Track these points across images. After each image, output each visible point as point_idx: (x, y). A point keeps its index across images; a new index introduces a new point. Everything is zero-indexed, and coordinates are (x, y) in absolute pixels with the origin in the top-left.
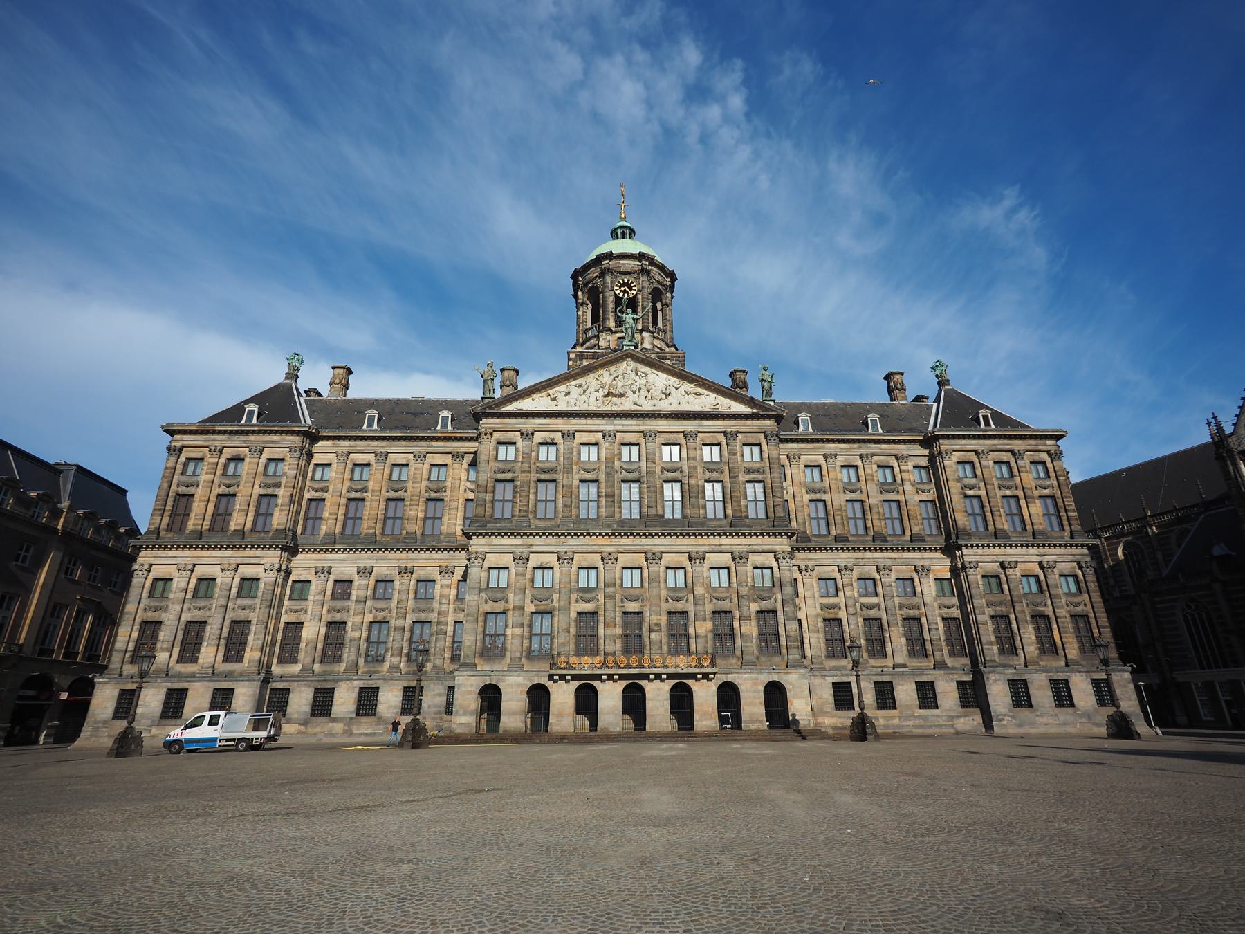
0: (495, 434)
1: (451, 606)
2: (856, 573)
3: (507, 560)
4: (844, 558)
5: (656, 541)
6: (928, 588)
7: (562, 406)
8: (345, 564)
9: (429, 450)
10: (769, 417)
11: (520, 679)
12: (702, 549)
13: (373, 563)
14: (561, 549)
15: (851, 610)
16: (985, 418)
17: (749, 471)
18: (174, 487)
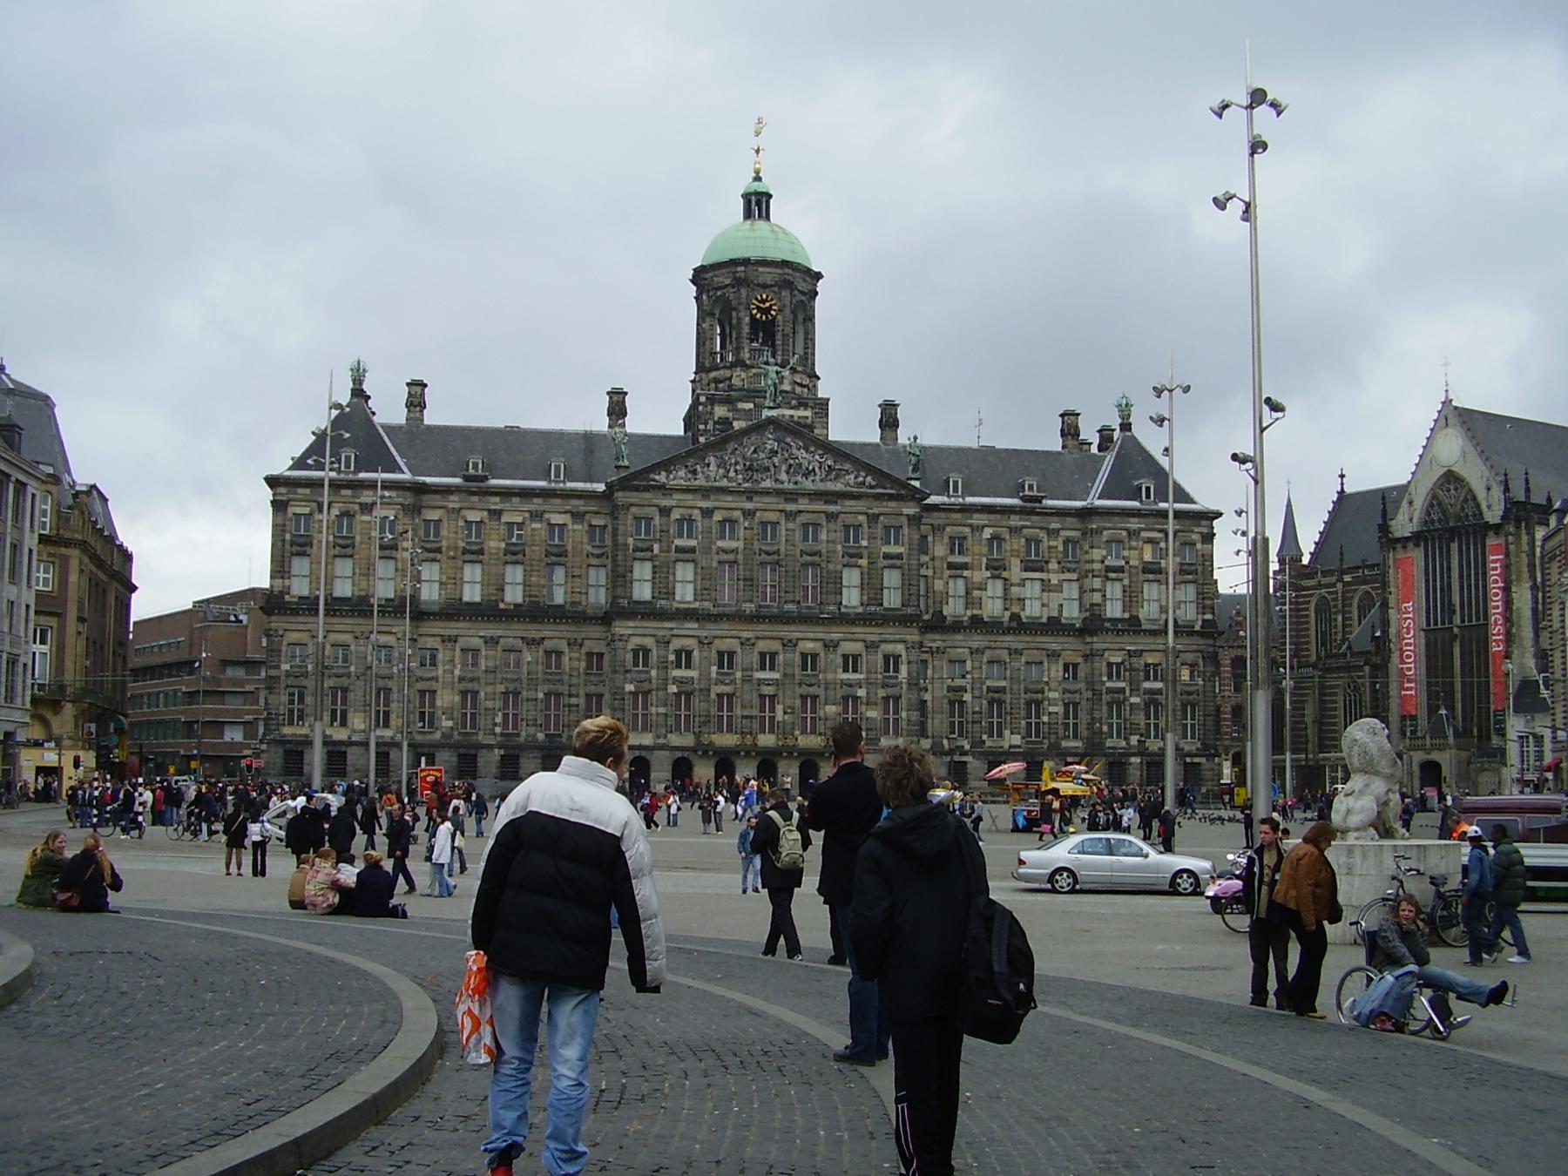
0: (633, 509)
1: (582, 677)
2: (987, 655)
3: (649, 642)
4: (977, 641)
5: (793, 628)
6: (1056, 671)
7: (701, 481)
8: (472, 634)
9: (545, 507)
10: (914, 498)
11: (667, 753)
12: (835, 636)
13: (500, 632)
14: (702, 633)
15: (977, 693)
16: (1148, 489)
17: (887, 556)
18: (287, 546)
